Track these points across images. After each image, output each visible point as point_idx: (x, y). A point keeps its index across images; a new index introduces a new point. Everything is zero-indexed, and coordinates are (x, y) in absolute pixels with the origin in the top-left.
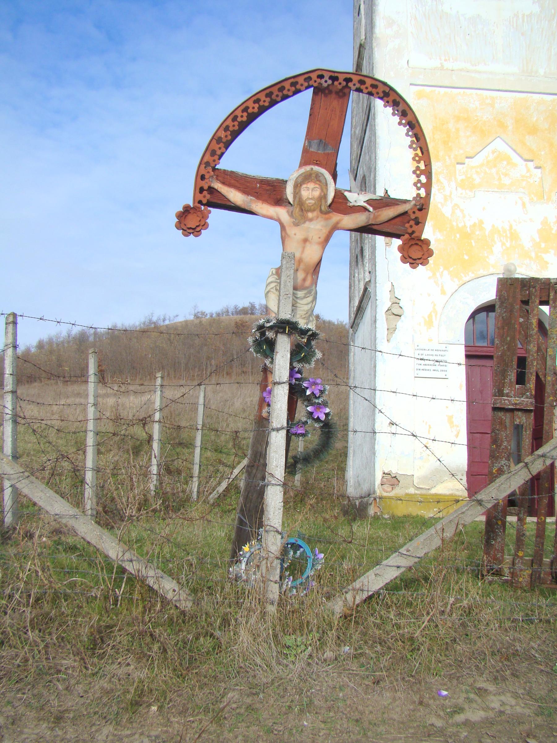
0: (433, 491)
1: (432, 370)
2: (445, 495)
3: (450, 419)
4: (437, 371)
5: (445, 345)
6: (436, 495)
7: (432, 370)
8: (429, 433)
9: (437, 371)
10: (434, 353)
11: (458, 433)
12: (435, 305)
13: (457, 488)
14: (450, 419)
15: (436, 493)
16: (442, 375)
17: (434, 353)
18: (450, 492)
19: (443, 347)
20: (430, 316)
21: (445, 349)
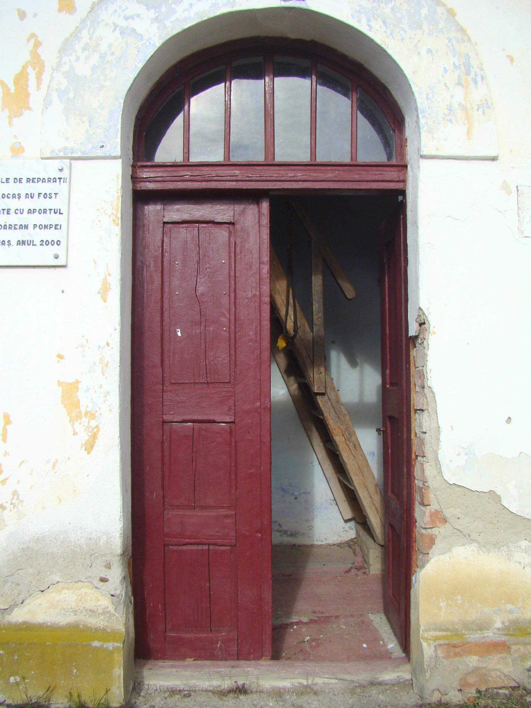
0: (18, 616)
1: (14, 242)
2: (53, 628)
3: (70, 392)
4: (31, 243)
5: (57, 164)
6: (27, 627)
7: (14, 242)
8: (5, 440)
9: (31, 243)
10: (24, 188)
11: (94, 436)
12: (38, 44)
13: (90, 605)
14: (70, 392)
15: (25, 623)
16: (45, 256)
17: (24, 188)
18: (71, 619)
19: (51, 169)
20: (21, 78)
21: (57, 175)
